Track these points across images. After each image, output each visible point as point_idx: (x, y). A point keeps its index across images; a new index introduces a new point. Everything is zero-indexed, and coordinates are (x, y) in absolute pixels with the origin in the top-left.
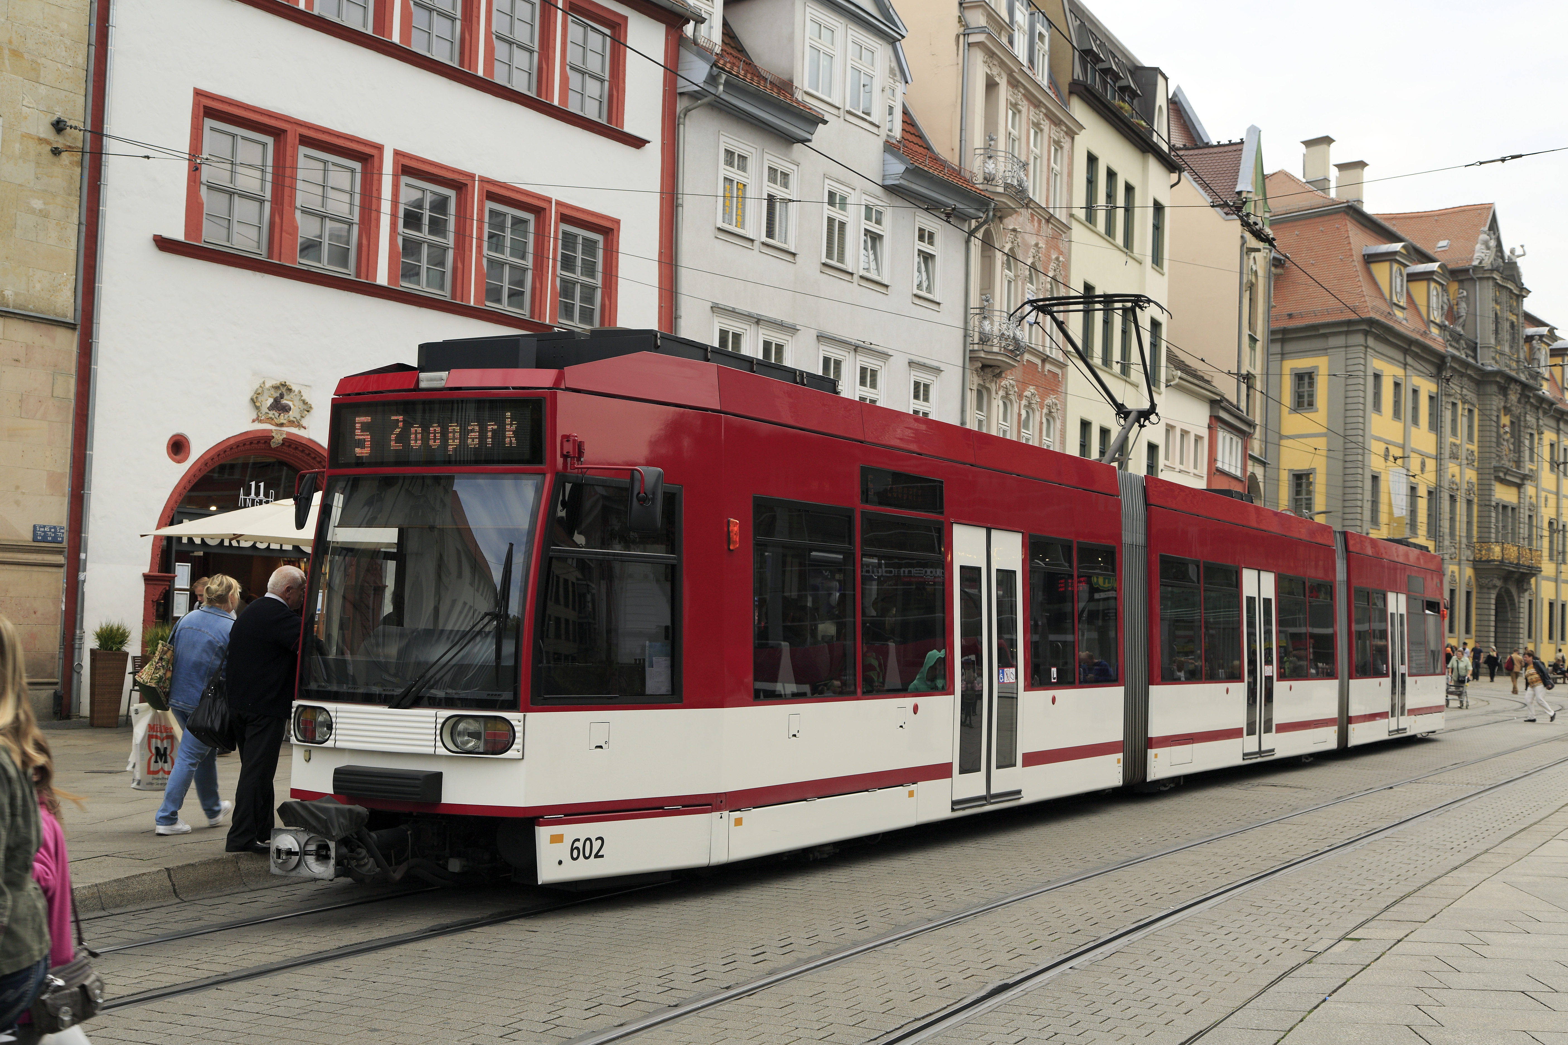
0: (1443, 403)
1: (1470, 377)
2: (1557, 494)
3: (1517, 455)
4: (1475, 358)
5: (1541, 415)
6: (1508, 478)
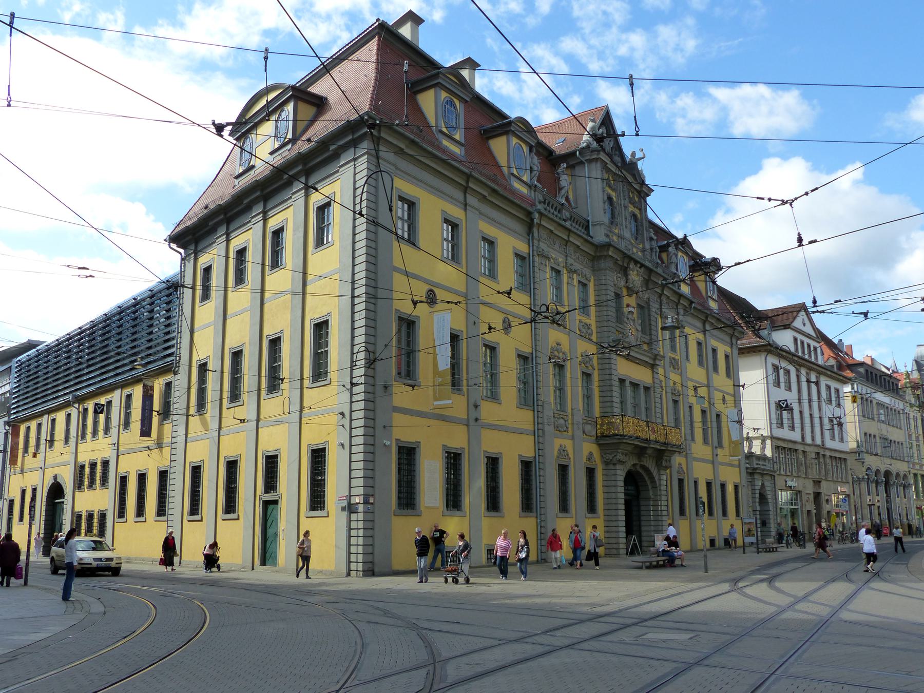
0: (536, 264)
3: (648, 337)
5: (681, 312)
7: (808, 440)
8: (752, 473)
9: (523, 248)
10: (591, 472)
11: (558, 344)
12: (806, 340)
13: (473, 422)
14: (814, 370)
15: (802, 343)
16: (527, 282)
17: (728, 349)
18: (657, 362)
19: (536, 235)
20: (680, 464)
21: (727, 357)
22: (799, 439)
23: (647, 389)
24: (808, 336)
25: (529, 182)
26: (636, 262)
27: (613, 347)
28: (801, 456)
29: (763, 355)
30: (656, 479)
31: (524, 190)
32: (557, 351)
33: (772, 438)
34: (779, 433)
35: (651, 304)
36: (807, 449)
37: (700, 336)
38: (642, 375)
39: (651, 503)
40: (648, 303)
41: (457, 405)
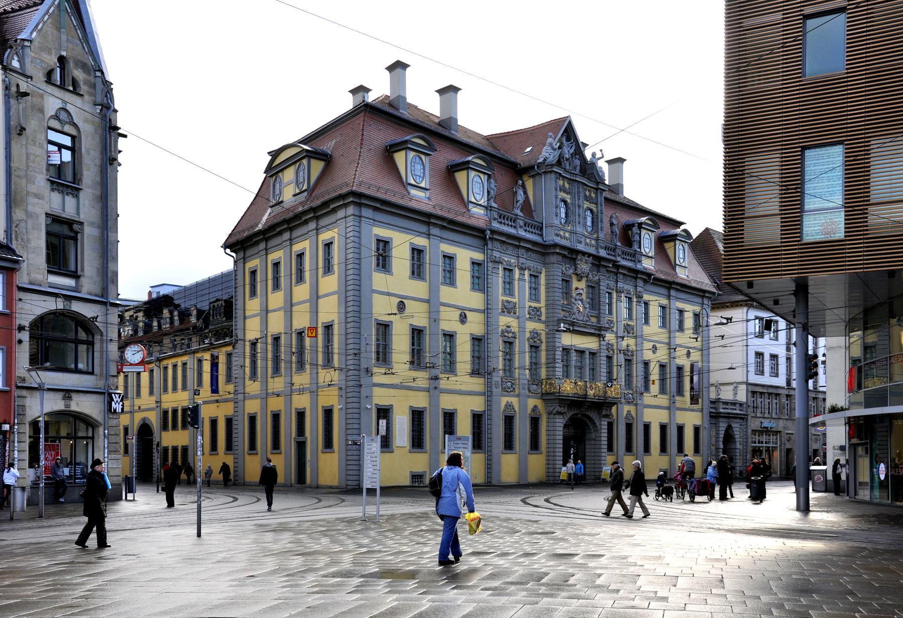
4: (541, 235)
5: (640, 283)
8: (715, 417)
10: (535, 422)
16: (480, 281)
17: (697, 309)
23: (593, 354)
28: (784, 400)
29: (745, 309)
32: (507, 332)
33: (748, 384)
34: (754, 379)
40: (598, 283)
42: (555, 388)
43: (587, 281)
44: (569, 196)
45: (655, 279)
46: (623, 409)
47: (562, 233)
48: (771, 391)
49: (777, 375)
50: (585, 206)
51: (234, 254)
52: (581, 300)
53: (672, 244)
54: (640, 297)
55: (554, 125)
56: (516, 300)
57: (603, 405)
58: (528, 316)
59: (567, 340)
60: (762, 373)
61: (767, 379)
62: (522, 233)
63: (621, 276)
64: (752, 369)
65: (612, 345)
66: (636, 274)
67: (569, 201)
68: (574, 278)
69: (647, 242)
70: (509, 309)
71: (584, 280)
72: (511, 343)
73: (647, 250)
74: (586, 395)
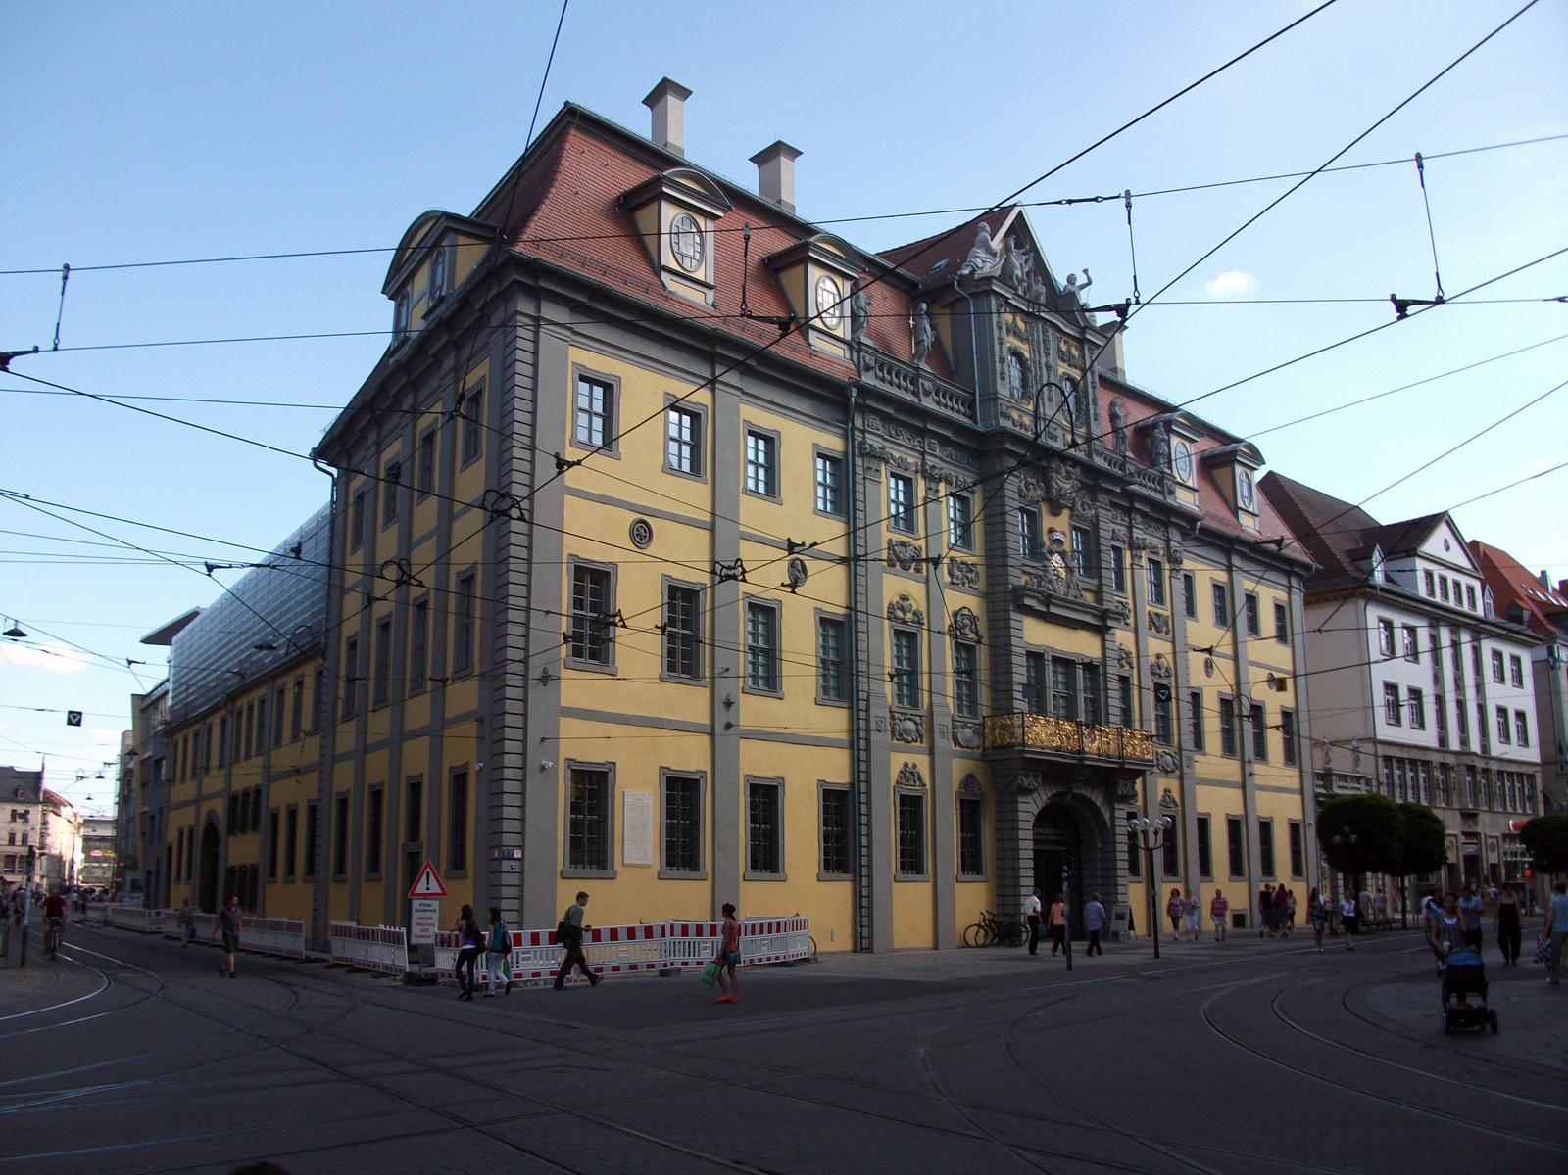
1: (944, 441)
2: (1236, 659)
3: (1095, 581)
5: (1175, 535)
6: (1053, 609)
7: (1454, 744)
9: (833, 443)
11: (904, 598)
12: (1451, 575)
13: (721, 729)
14: (1466, 626)
15: (1443, 580)
16: (844, 498)
17: (1282, 596)
18: (1110, 623)
19: (858, 423)
20: (1167, 791)
21: (1279, 609)
22: (1434, 743)
23: (1090, 667)
24: (1459, 570)
25: (848, 337)
26: (1062, 457)
27: (1005, 600)
30: (1107, 816)
31: (838, 351)
32: (902, 609)
35: (1101, 525)
36: (1451, 760)
37: (1222, 576)
38: (1082, 645)
39: (1098, 856)
40: (1095, 525)
41: (691, 702)
42: (1012, 735)
43: (1071, 517)
44: (1026, 347)
45: (1204, 530)
46: (1155, 786)
47: (1015, 415)
48: (1415, 755)
49: (1422, 726)
50: (1061, 371)
51: (334, 471)
52: (1063, 554)
53: (1227, 470)
54: (1175, 561)
55: (994, 216)
56: (922, 543)
57: (1117, 778)
58: (947, 579)
59: (1034, 634)
60: (1398, 722)
61: (1405, 734)
62: (928, 403)
63: (1138, 518)
64: (1380, 714)
65: (1128, 654)
66: (1166, 516)
67: (1027, 355)
68: (1044, 508)
69: (1183, 456)
70: (902, 560)
71: (1066, 513)
72: (912, 637)
73: (1184, 475)
74: (1081, 751)
